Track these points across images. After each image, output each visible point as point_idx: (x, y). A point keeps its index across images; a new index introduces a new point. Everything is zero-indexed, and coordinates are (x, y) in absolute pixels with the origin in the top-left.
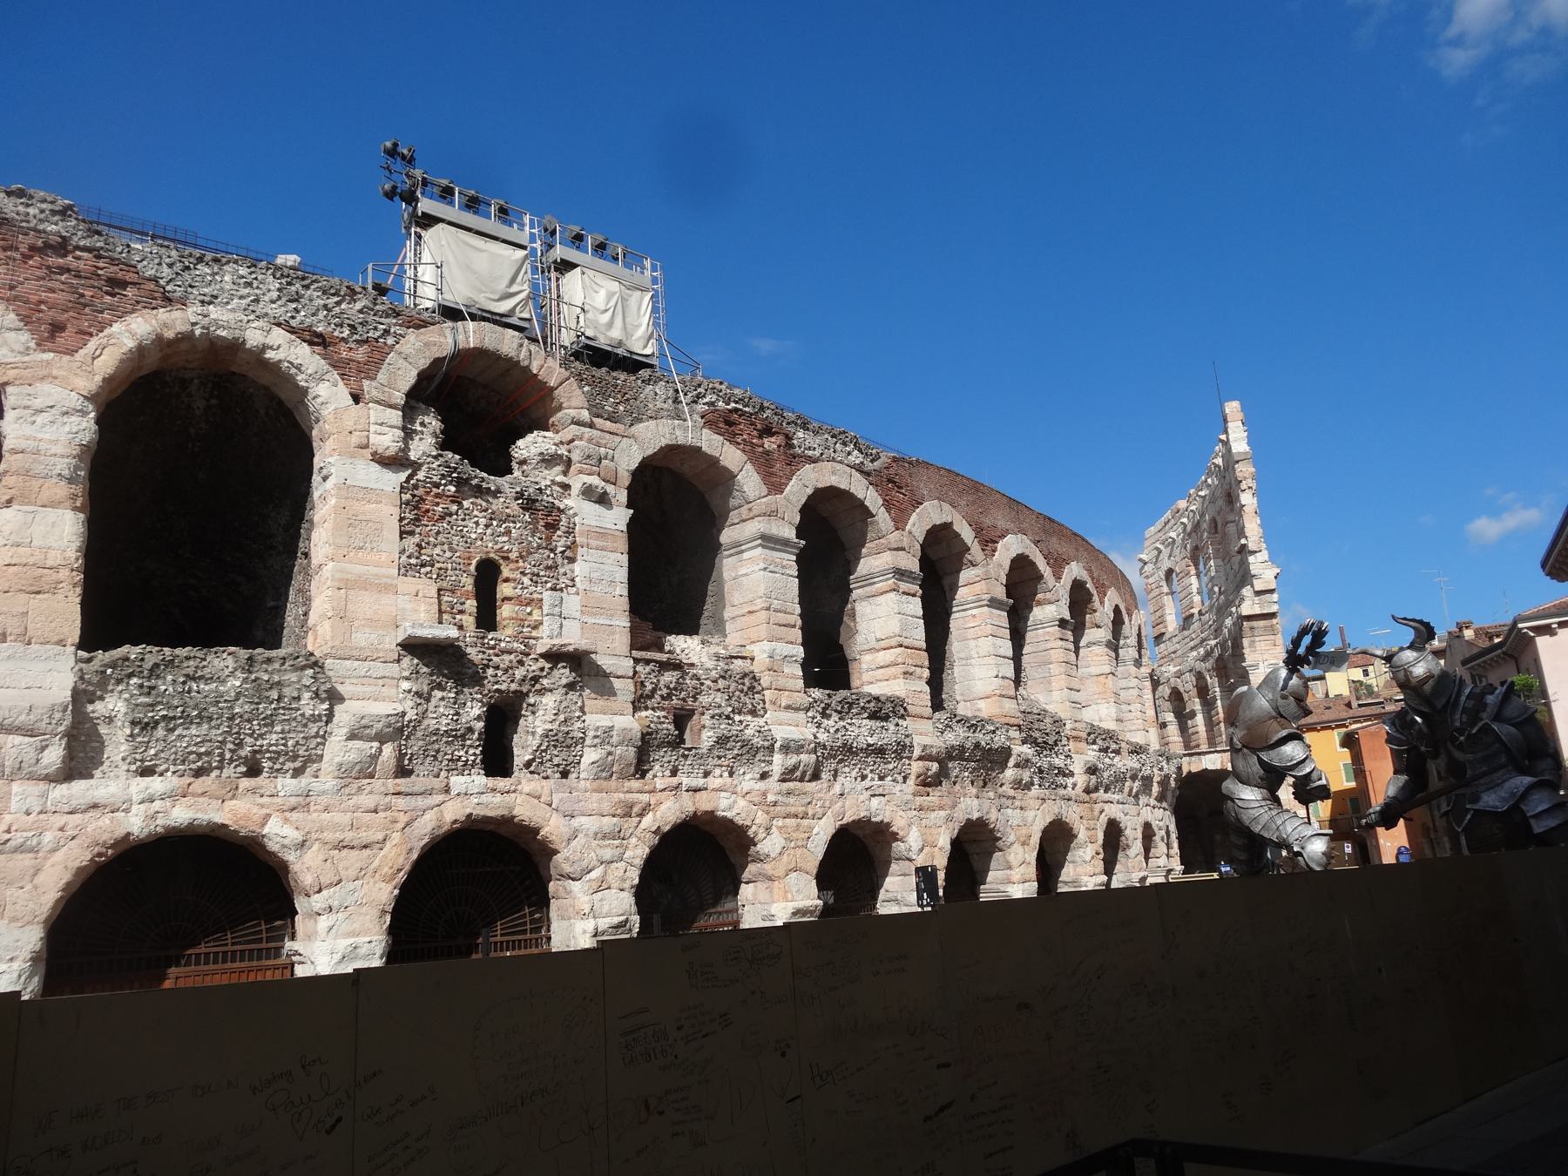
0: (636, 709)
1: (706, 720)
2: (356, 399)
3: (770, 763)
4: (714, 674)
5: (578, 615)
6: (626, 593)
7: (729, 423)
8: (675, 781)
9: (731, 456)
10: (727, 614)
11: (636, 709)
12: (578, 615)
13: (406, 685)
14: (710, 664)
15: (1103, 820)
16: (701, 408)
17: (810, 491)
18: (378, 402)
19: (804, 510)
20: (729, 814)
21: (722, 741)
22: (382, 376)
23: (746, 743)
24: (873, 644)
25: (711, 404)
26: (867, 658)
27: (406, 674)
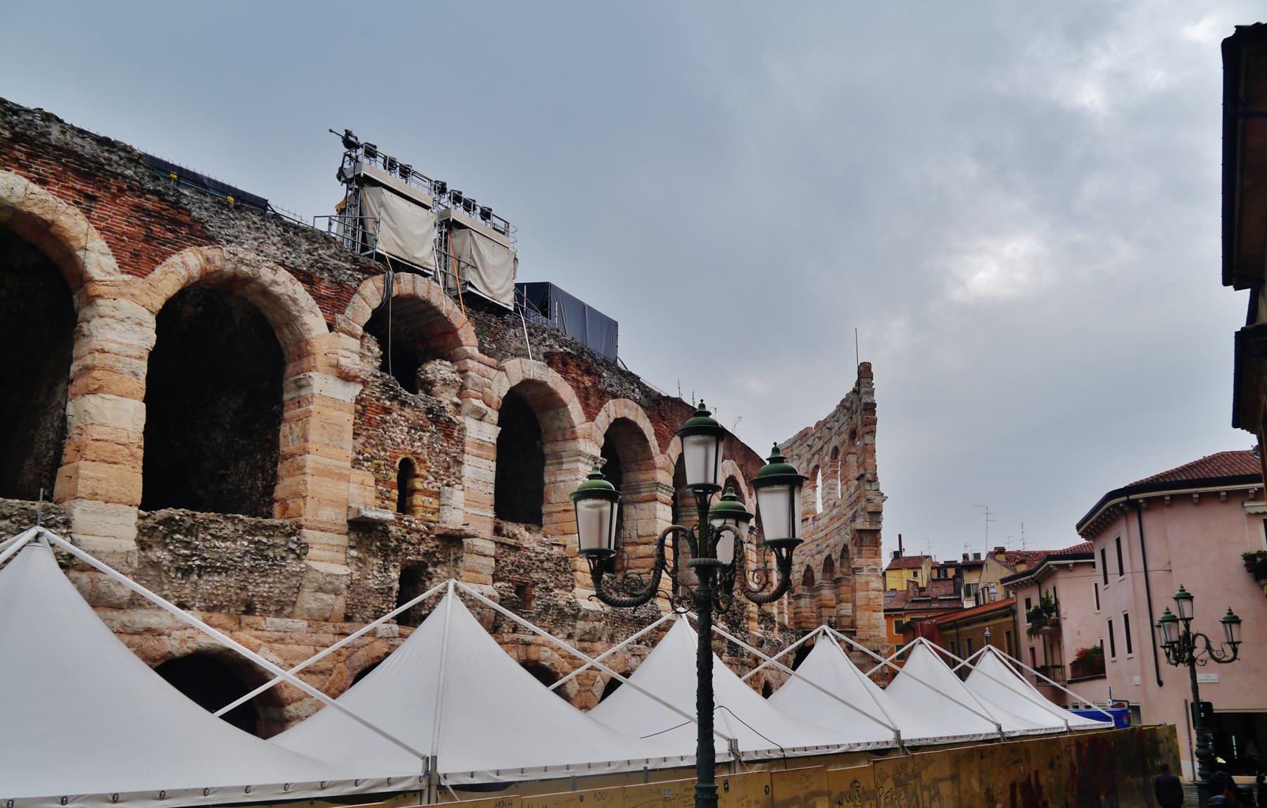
0: (494, 581)
1: (536, 592)
2: (331, 327)
3: (574, 627)
4: (542, 557)
5: (462, 506)
6: (492, 491)
7: (565, 364)
8: (516, 636)
9: (566, 391)
10: (545, 509)
11: (494, 581)
12: (462, 506)
13: (354, 553)
14: (539, 549)
15: (763, 681)
16: (543, 349)
17: (612, 420)
18: (343, 332)
19: (607, 436)
20: (547, 664)
21: (547, 608)
22: (348, 312)
23: (561, 611)
24: (635, 538)
25: (551, 346)
26: (629, 549)
27: (352, 544)
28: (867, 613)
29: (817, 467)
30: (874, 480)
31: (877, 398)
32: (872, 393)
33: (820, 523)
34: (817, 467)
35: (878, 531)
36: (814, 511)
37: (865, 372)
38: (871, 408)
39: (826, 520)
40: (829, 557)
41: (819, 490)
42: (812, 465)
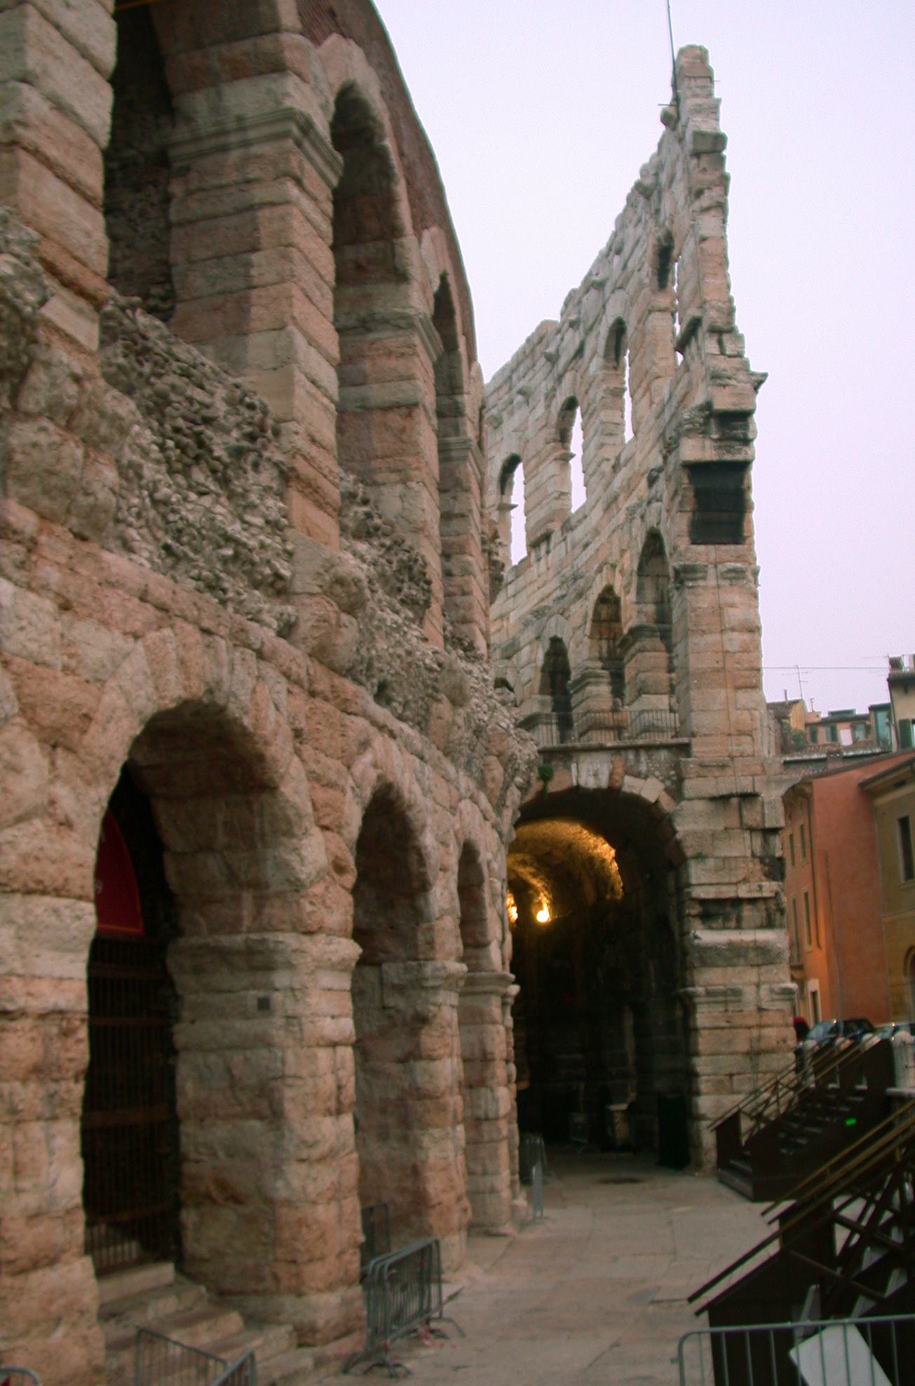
28: (722, 694)
29: (571, 405)
30: (725, 331)
31: (726, 124)
32: (713, 110)
33: (579, 534)
34: (571, 405)
35: (744, 466)
36: (565, 510)
37: (692, 71)
38: (711, 148)
39: (597, 514)
40: (608, 598)
41: (576, 465)
42: (560, 400)
